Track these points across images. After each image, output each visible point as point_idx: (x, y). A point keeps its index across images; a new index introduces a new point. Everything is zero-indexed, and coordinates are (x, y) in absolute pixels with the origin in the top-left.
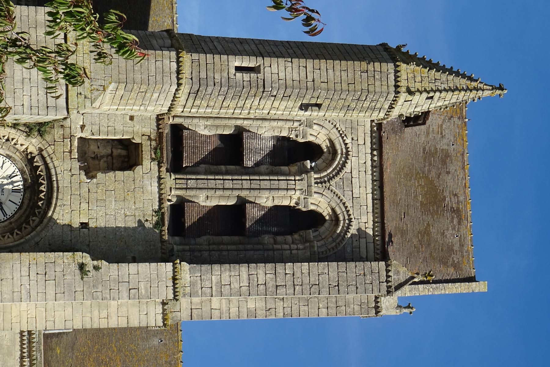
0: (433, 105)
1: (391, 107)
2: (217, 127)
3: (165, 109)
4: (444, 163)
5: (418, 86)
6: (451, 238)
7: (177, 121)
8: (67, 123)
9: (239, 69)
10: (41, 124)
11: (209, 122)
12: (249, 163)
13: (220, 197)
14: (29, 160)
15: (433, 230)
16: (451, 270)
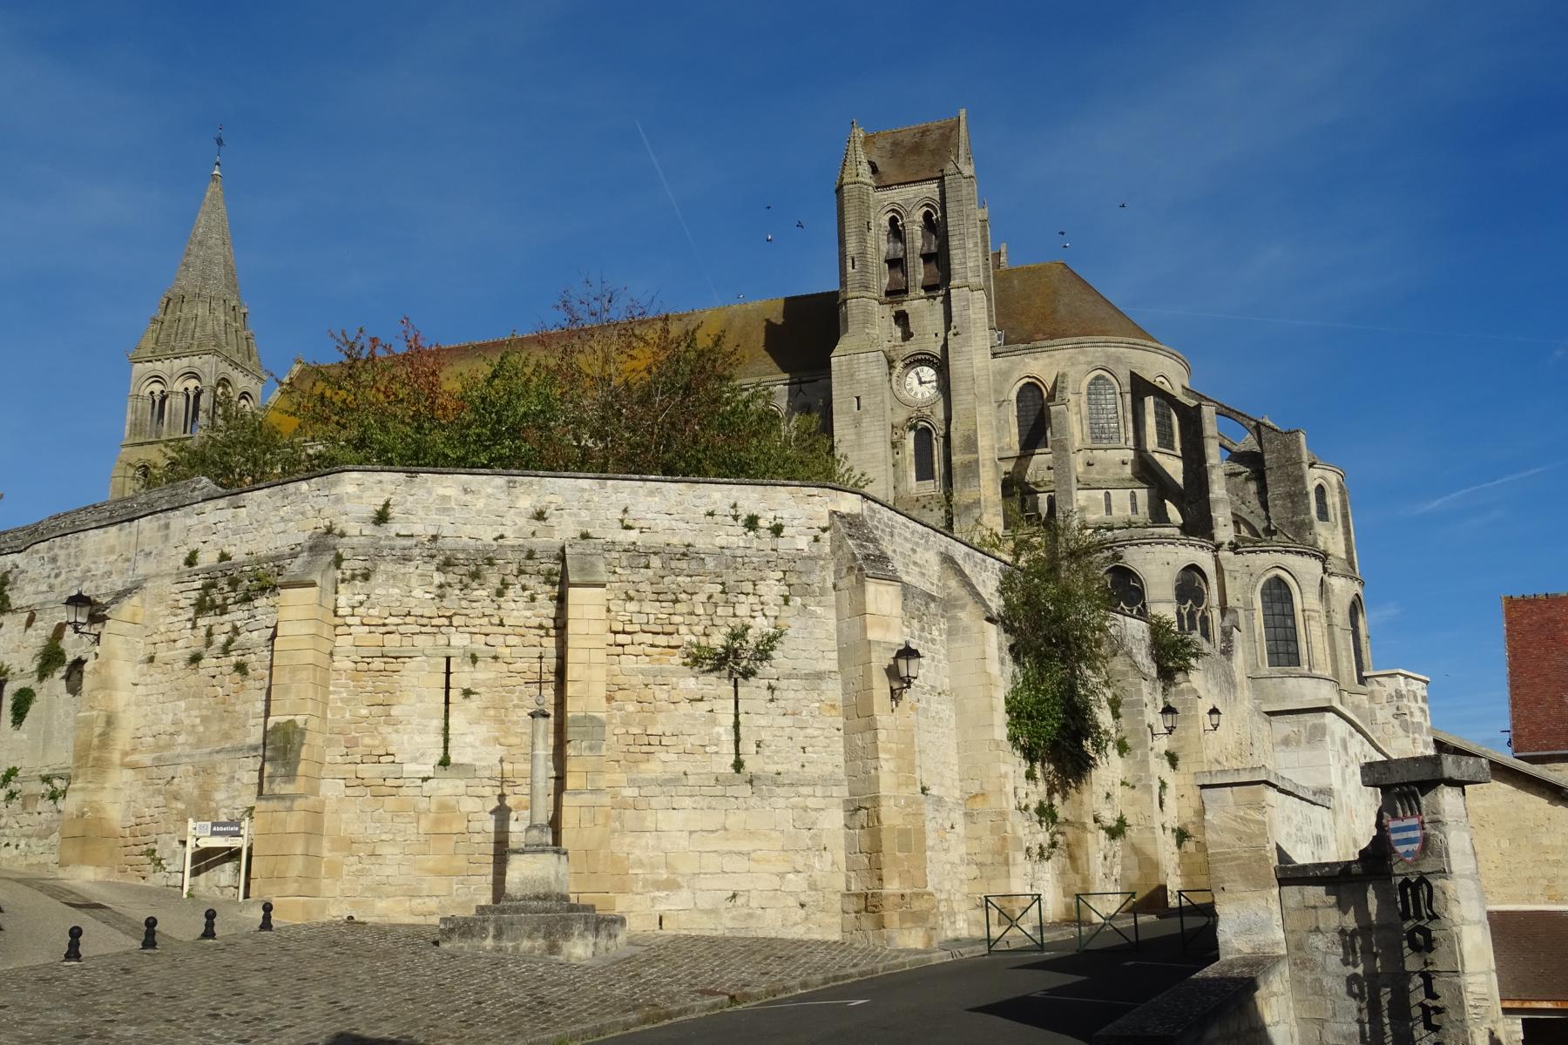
0: (864, 159)
1: (866, 184)
2: (885, 273)
3: (876, 302)
4: (898, 144)
5: (854, 171)
6: (936, 135)
7: (883, 294)
8: (886, 349)
9: (853, 268)
10: (888, 362)
11: (883, 277)
12: (901, 254)
13: (919, 267)
14: (906, 366)
15: (932, 147)
16: (953, 133)
